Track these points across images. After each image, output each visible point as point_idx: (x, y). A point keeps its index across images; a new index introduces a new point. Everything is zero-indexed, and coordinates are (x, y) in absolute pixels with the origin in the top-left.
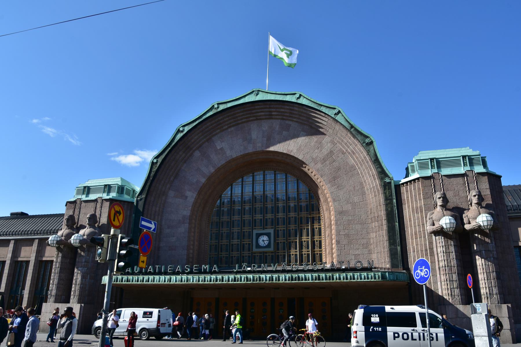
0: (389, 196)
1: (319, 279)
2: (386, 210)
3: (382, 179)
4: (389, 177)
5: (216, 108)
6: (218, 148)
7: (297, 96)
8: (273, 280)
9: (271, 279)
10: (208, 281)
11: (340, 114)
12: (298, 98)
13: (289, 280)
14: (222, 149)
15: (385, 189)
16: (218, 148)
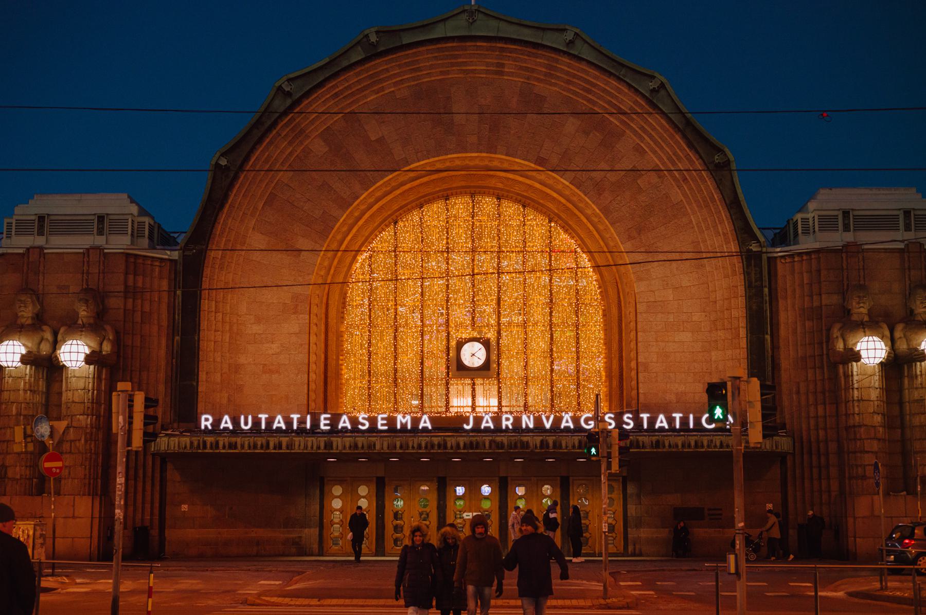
0: (756, 281)
1: (638, 447)
2: (749, 308)
3: (742, 243)
4: (759, 241)
5: (372, 44)
6: (373, 139)
7: (569, 36)
8: (548, 447)
9: (544, 444)
10: (413, 447)
11: (663, 92)
12: (571, 42)
13: (580, 447)
14: (381, 140)
15: (749, 265)
16: (373, 139)
